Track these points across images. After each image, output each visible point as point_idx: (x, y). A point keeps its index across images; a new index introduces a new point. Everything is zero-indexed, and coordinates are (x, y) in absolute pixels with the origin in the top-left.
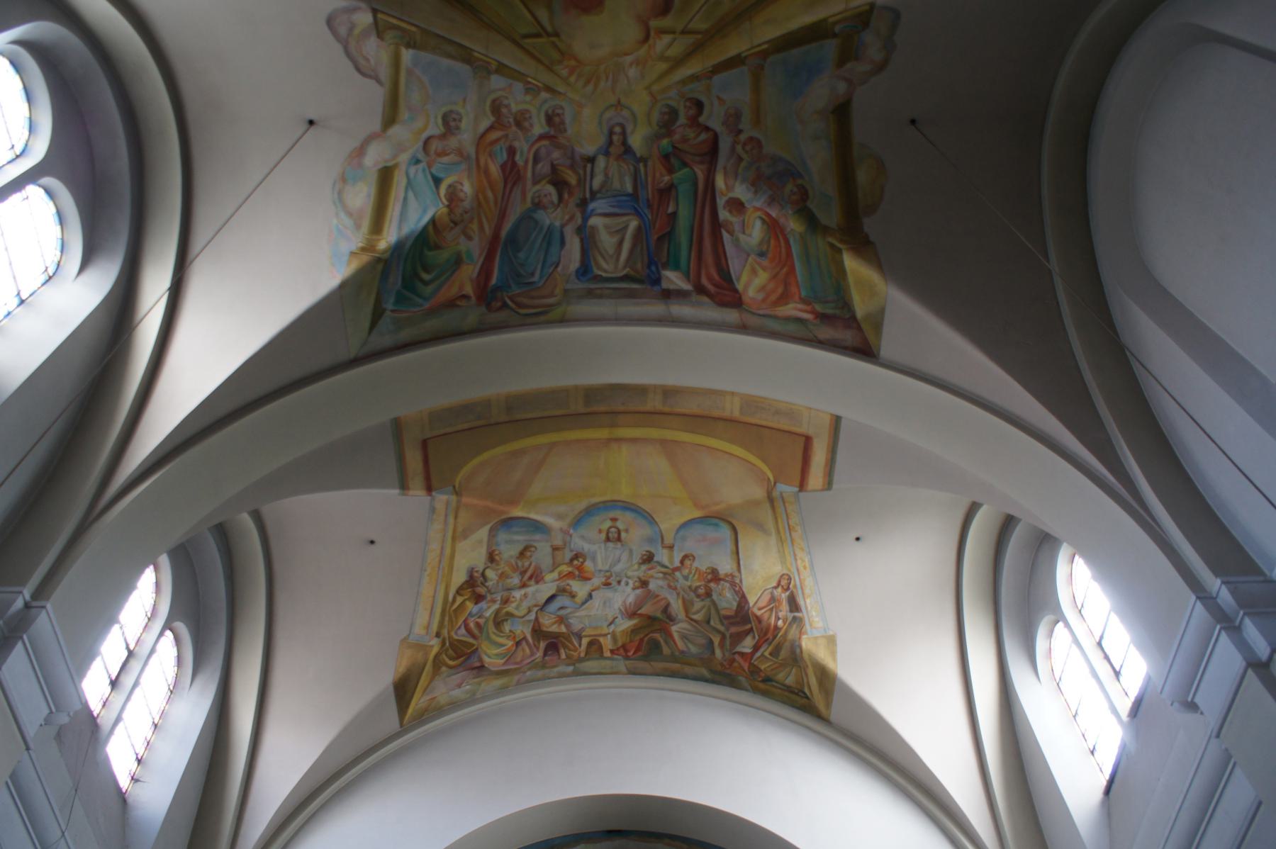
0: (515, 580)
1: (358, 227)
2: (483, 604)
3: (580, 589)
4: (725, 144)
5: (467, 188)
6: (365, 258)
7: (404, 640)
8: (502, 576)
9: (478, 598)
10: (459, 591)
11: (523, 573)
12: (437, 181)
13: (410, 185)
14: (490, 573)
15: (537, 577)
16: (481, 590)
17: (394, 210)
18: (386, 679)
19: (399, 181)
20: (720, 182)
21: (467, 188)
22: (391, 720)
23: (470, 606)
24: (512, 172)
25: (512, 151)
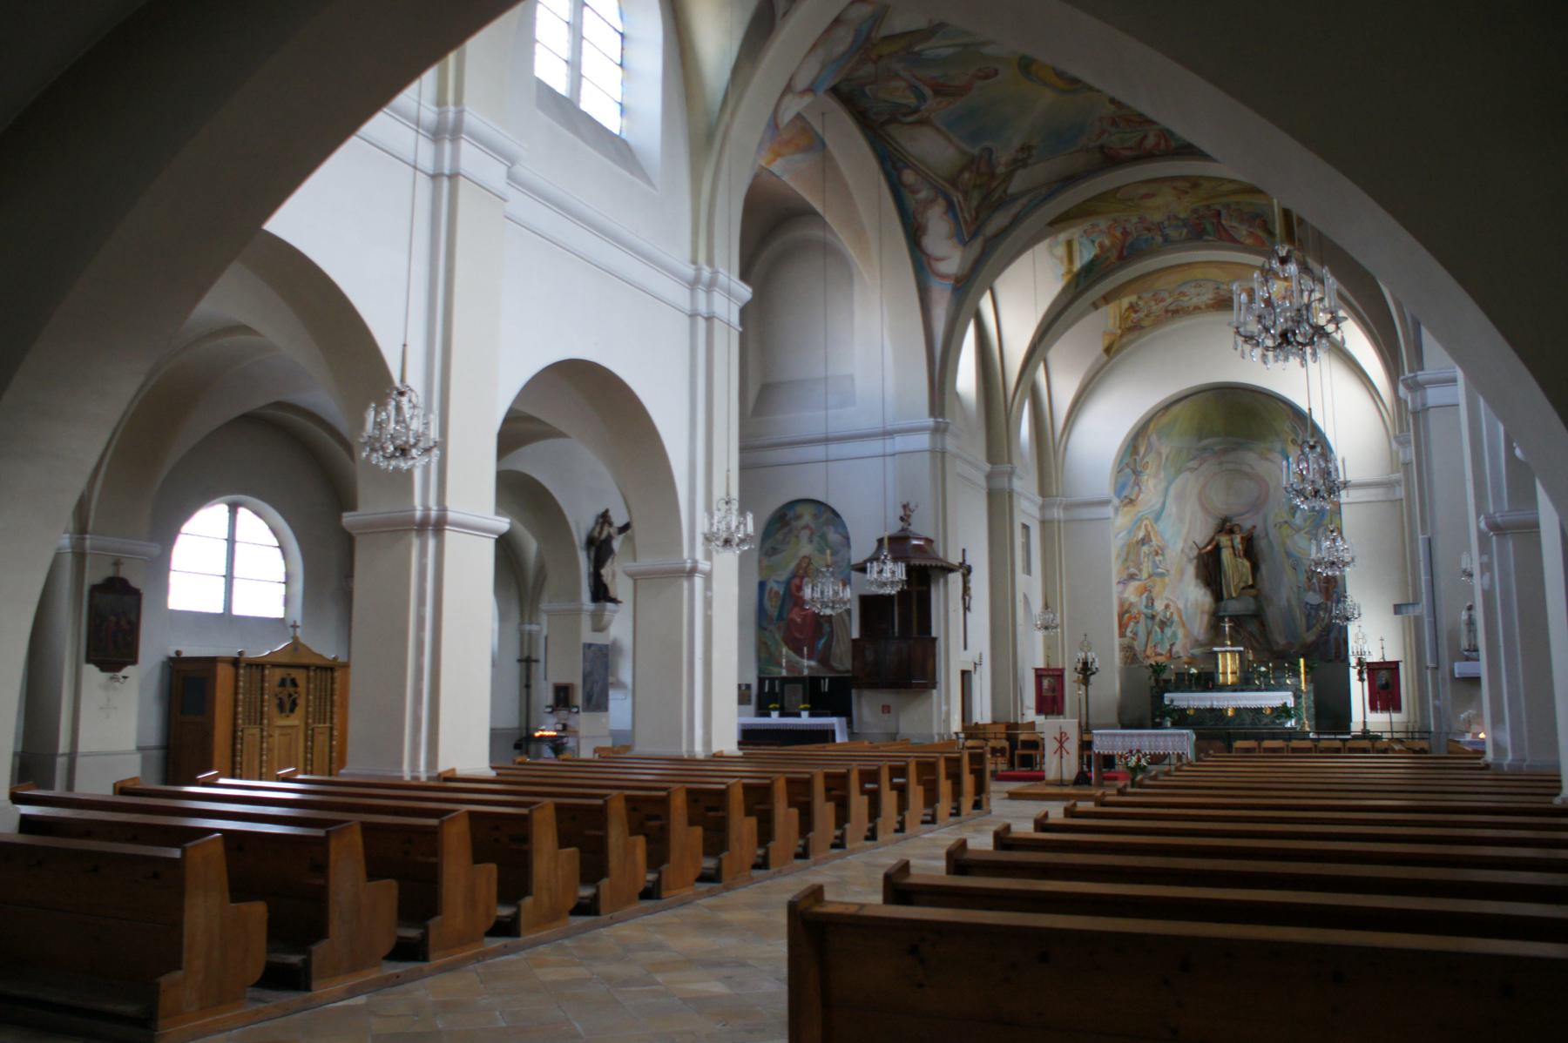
0: (1153, 303)
1: (1062, 262)
2: (1138, 314)
3: (1186, 299)
4: (1224, 212)
5: (1107, 242)
6: (1069, 276)
7: (1104, 332)
8: (1146, 303)
9: (1136, 312)
10: (1127, 310)
11: (1156, 300)
12: (1093, 242)
13: (1081, 244)
14: (1140, 303)
15: (1163, 300)
16: (1137, 309)
17: (1076, 255)
18: (1100, 349)
19: (1076, 246)
20: (1224, 222)
21: (1107, 242)
22: (1105, 358)
23: (1134, 315)
24: (1125, 233)
25: (1124, 228)
